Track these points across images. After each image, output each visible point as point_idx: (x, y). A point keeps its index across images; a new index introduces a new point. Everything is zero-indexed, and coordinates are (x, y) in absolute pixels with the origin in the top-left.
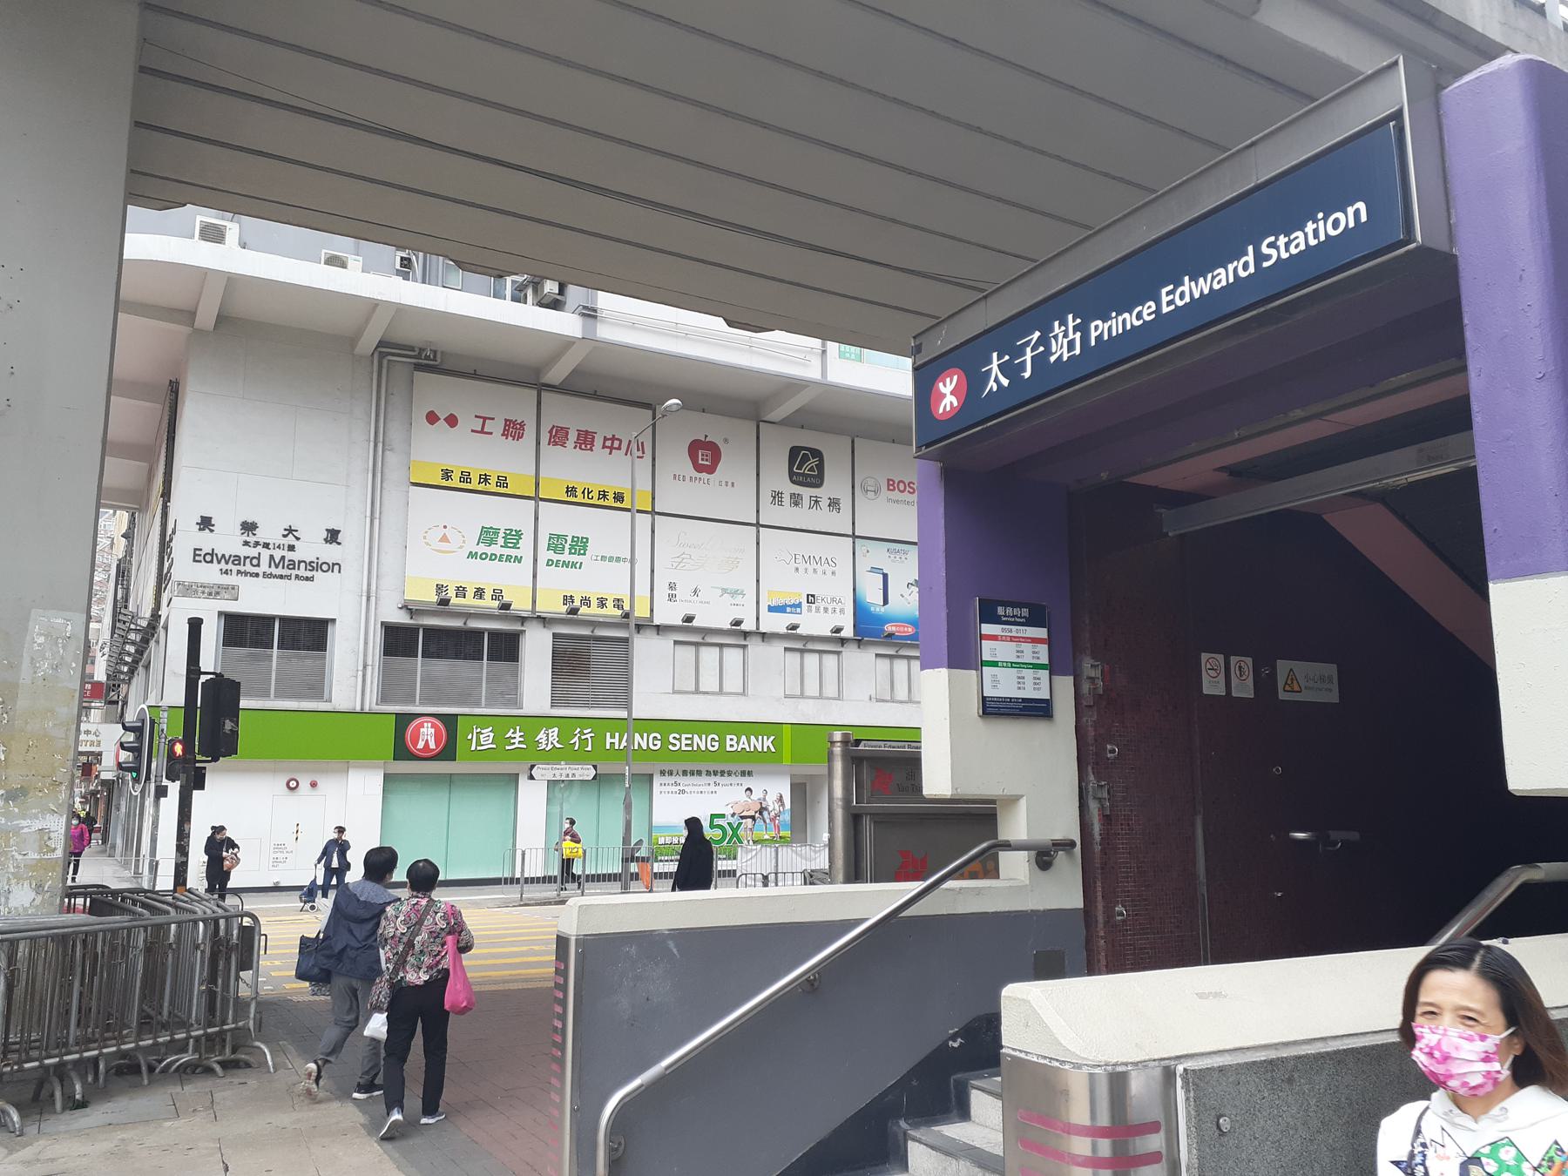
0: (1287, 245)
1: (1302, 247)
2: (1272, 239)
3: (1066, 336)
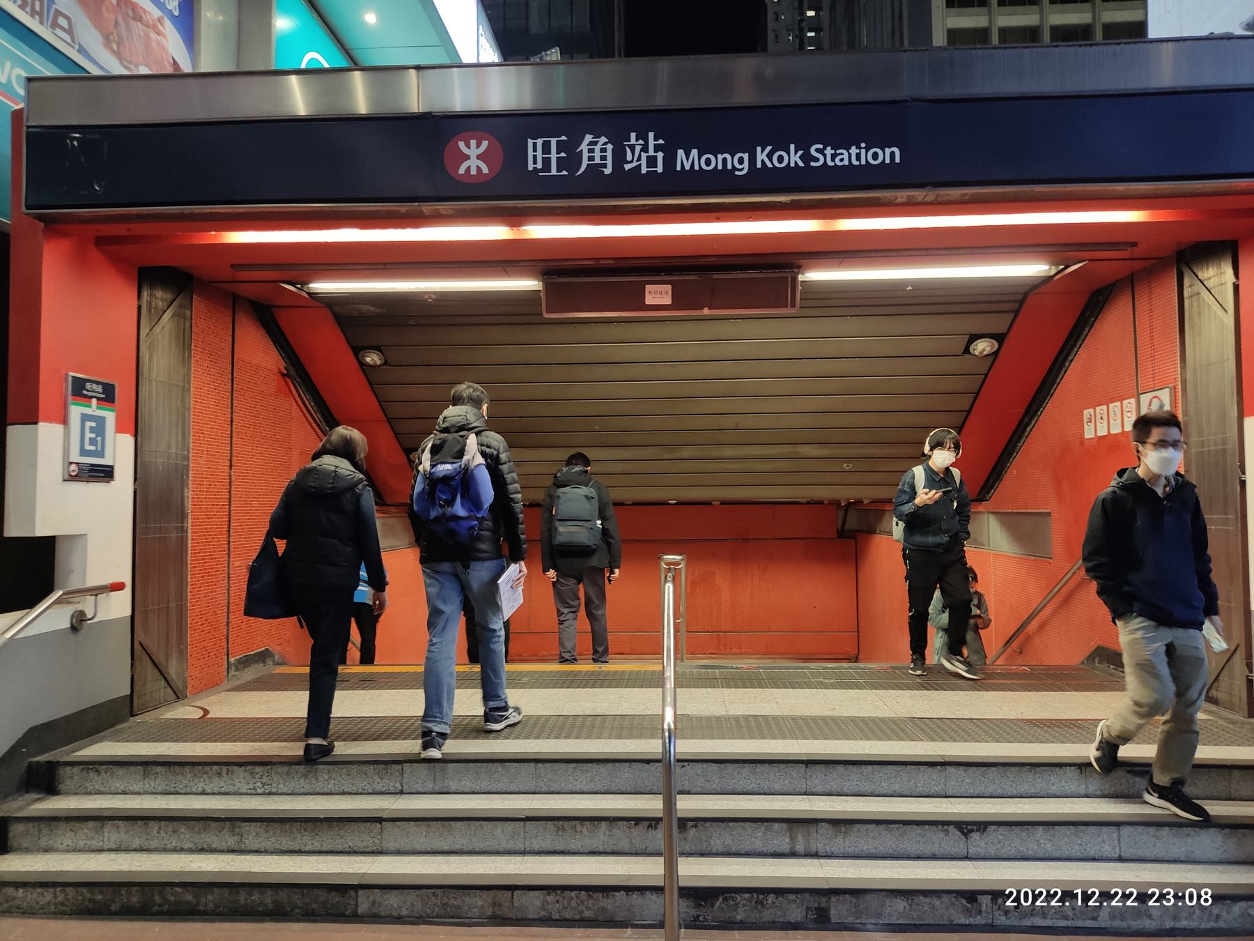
0: (833, 157)
1: (846, 162)
2: (821, 146)
3: (645, 149)
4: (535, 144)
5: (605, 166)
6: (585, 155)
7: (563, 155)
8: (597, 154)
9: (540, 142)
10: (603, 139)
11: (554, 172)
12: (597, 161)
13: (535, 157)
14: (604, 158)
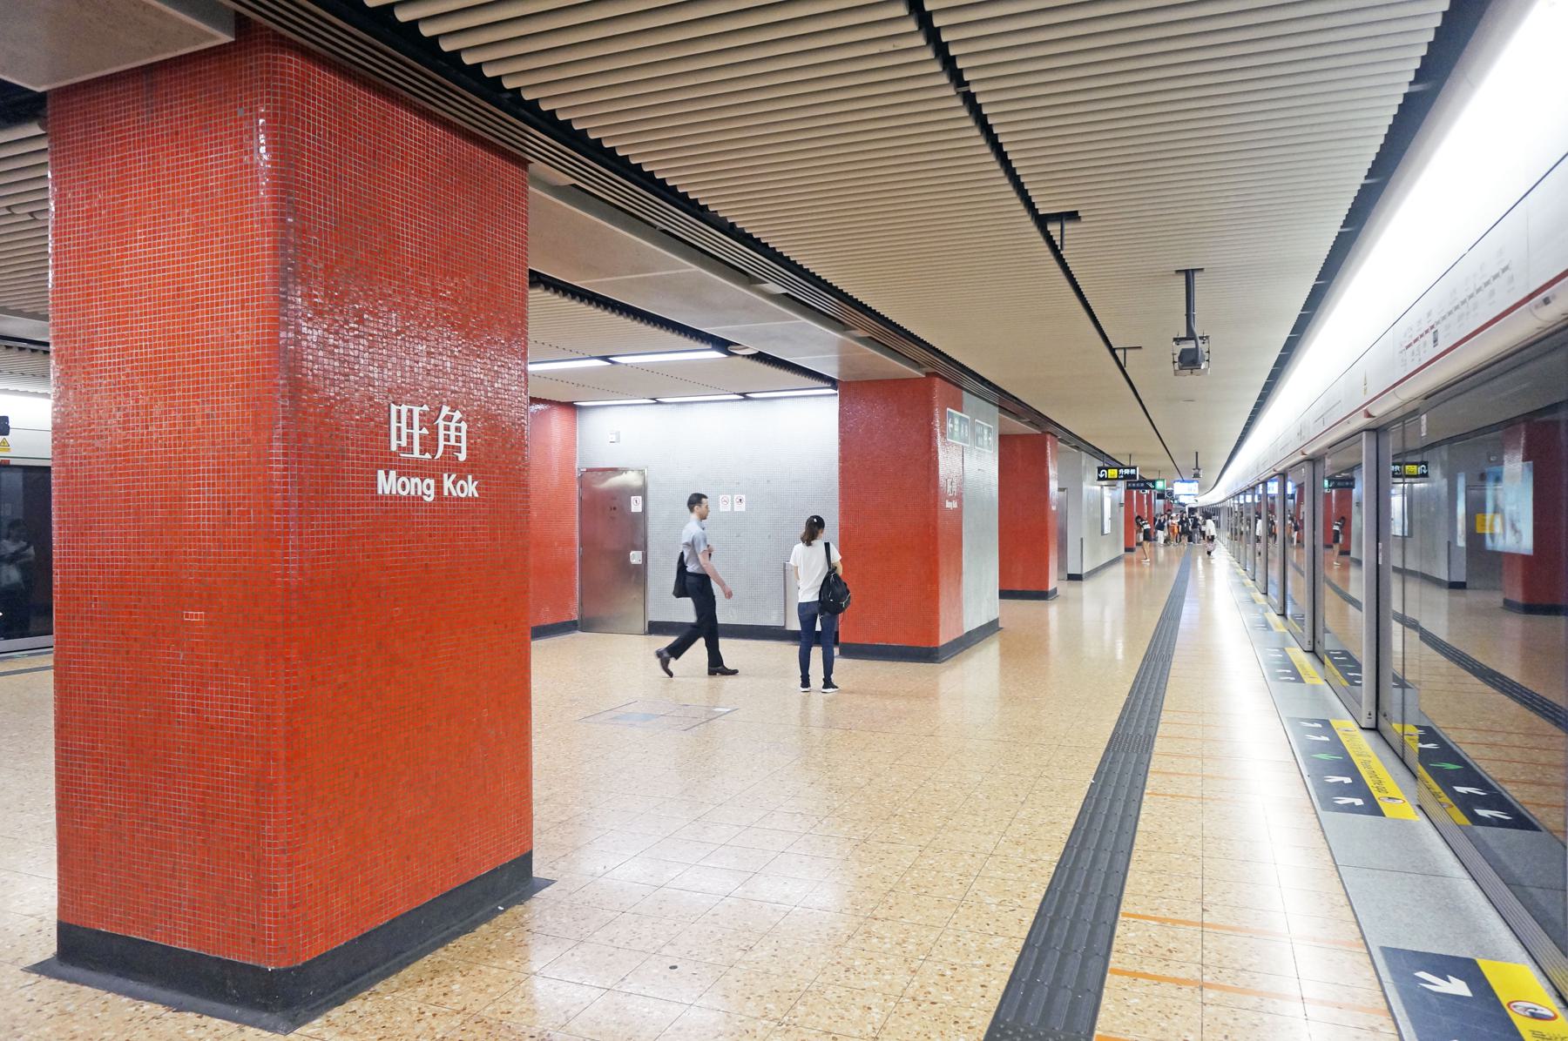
4: (399, 412)
5: (459, 450)
6: (441, 432)
7: (425, 431)
8: (453, 433)
9: (404, 408)
10: (457, 415)
11: (416, 454)
12: (453, 442)
13: (399, 429)
14: (458, 439)
